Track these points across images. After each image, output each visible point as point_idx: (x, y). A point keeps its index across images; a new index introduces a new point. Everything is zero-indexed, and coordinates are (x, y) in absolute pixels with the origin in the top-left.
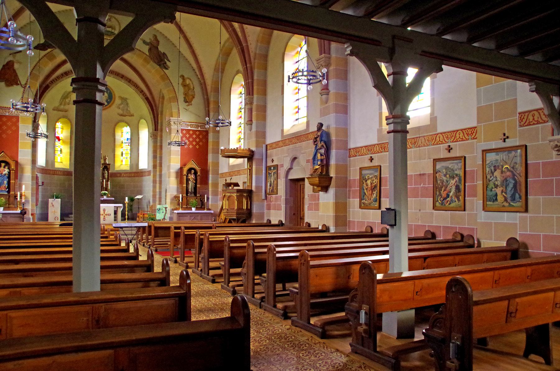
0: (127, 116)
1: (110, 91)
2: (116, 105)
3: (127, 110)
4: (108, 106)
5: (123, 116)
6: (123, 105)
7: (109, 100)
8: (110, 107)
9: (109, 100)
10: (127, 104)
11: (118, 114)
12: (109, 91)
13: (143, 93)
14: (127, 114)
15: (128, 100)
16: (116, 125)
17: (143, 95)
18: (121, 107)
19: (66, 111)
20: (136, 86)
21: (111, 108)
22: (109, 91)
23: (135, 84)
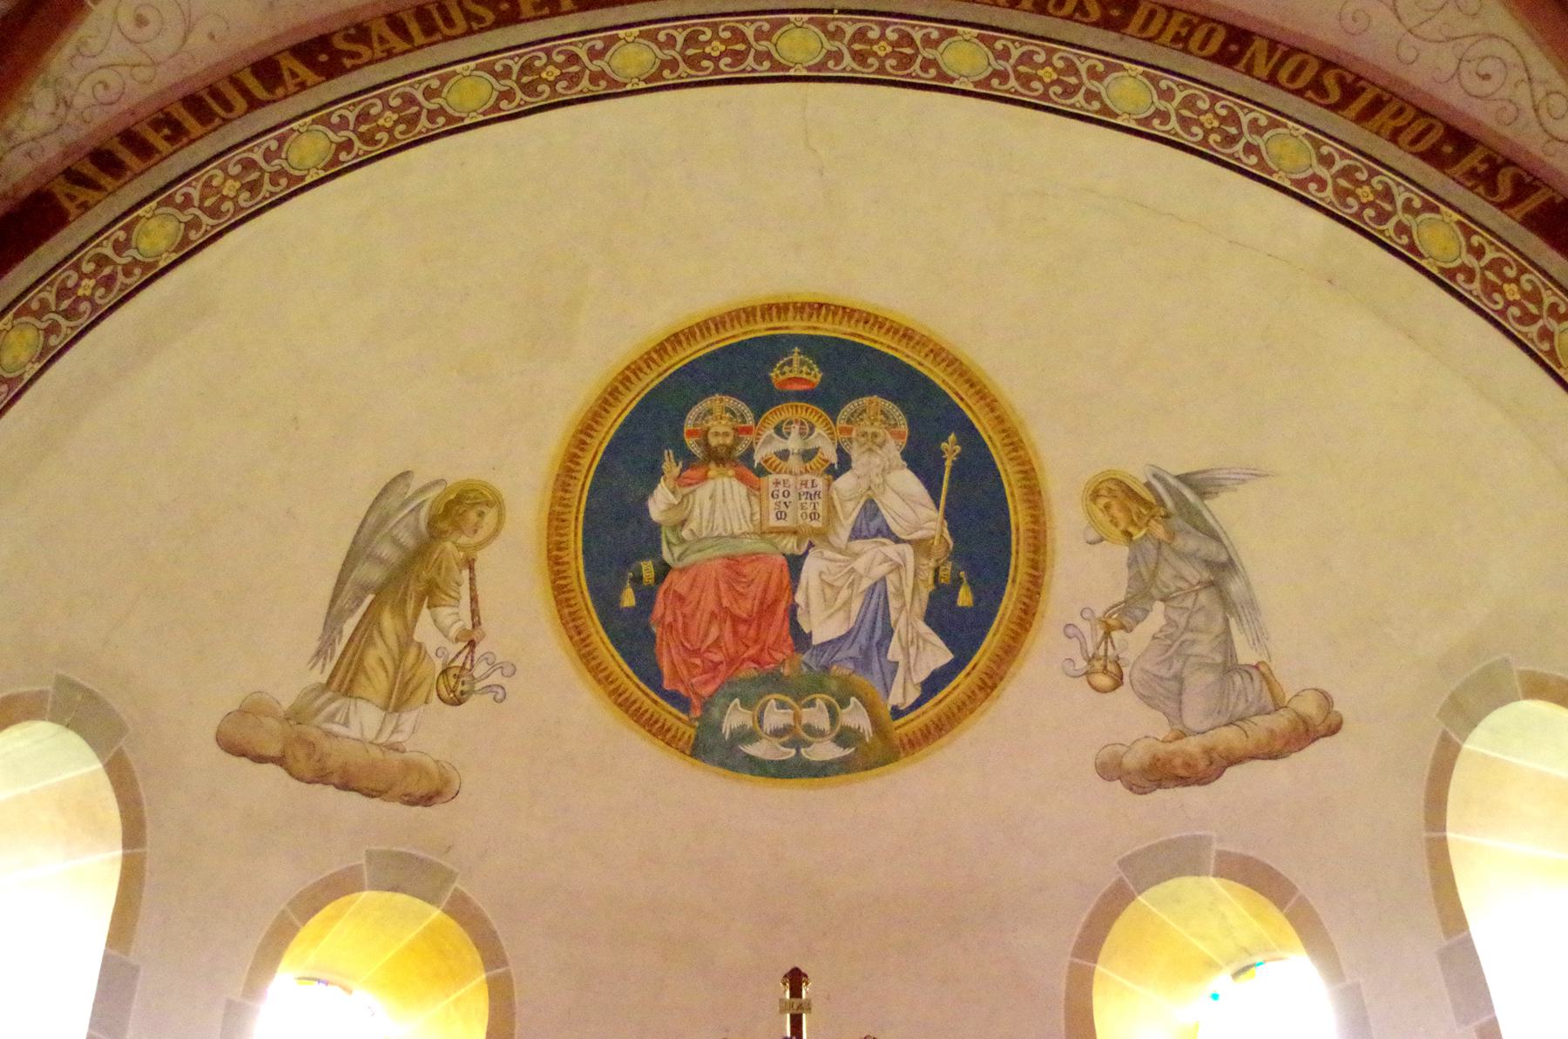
0: (1234, 760)
1: (968, 432)
2: (1069, 630)
3: (1229, 667)
4: (963, 682)
5: (1183, 781)
6: (1157, 617)
7: (965, 598)
8: (989, 685)
9: (965, 598)
10: (1221, 570)
11: (1110, 770)
12: (951, 448)
13: (1473, 160)
14: (1229, 737)
15: (1219, 509)
16: (1090, 944)
17: (1485, 180)
18: (1134, 645)
19: (427, 800)
20: (1350, 92)
21: (1011, 693)
22: (951, 448)
23: (1327, 64)
